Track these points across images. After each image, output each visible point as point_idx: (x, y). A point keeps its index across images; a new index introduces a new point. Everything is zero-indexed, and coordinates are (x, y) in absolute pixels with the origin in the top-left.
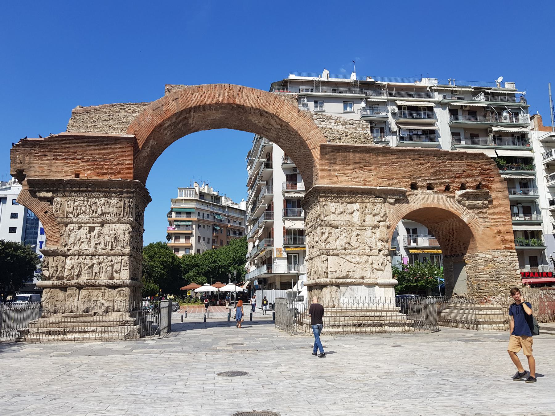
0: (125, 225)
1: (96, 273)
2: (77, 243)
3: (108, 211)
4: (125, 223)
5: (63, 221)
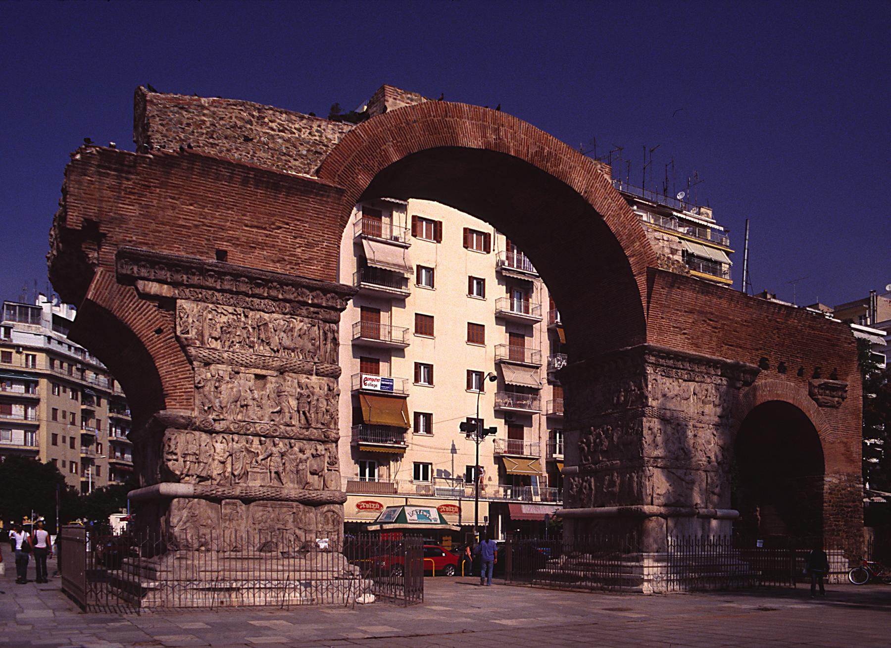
0: (325, 378)
3: (292, 346)
4: (327, 376)
5: (201, 356)
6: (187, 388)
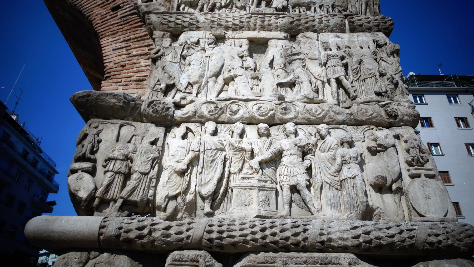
0: (368, 34)
1: (294, 189)
2: (211, 83)
4: (370, 30)
5: (165, 22)
6: (141, 67)
